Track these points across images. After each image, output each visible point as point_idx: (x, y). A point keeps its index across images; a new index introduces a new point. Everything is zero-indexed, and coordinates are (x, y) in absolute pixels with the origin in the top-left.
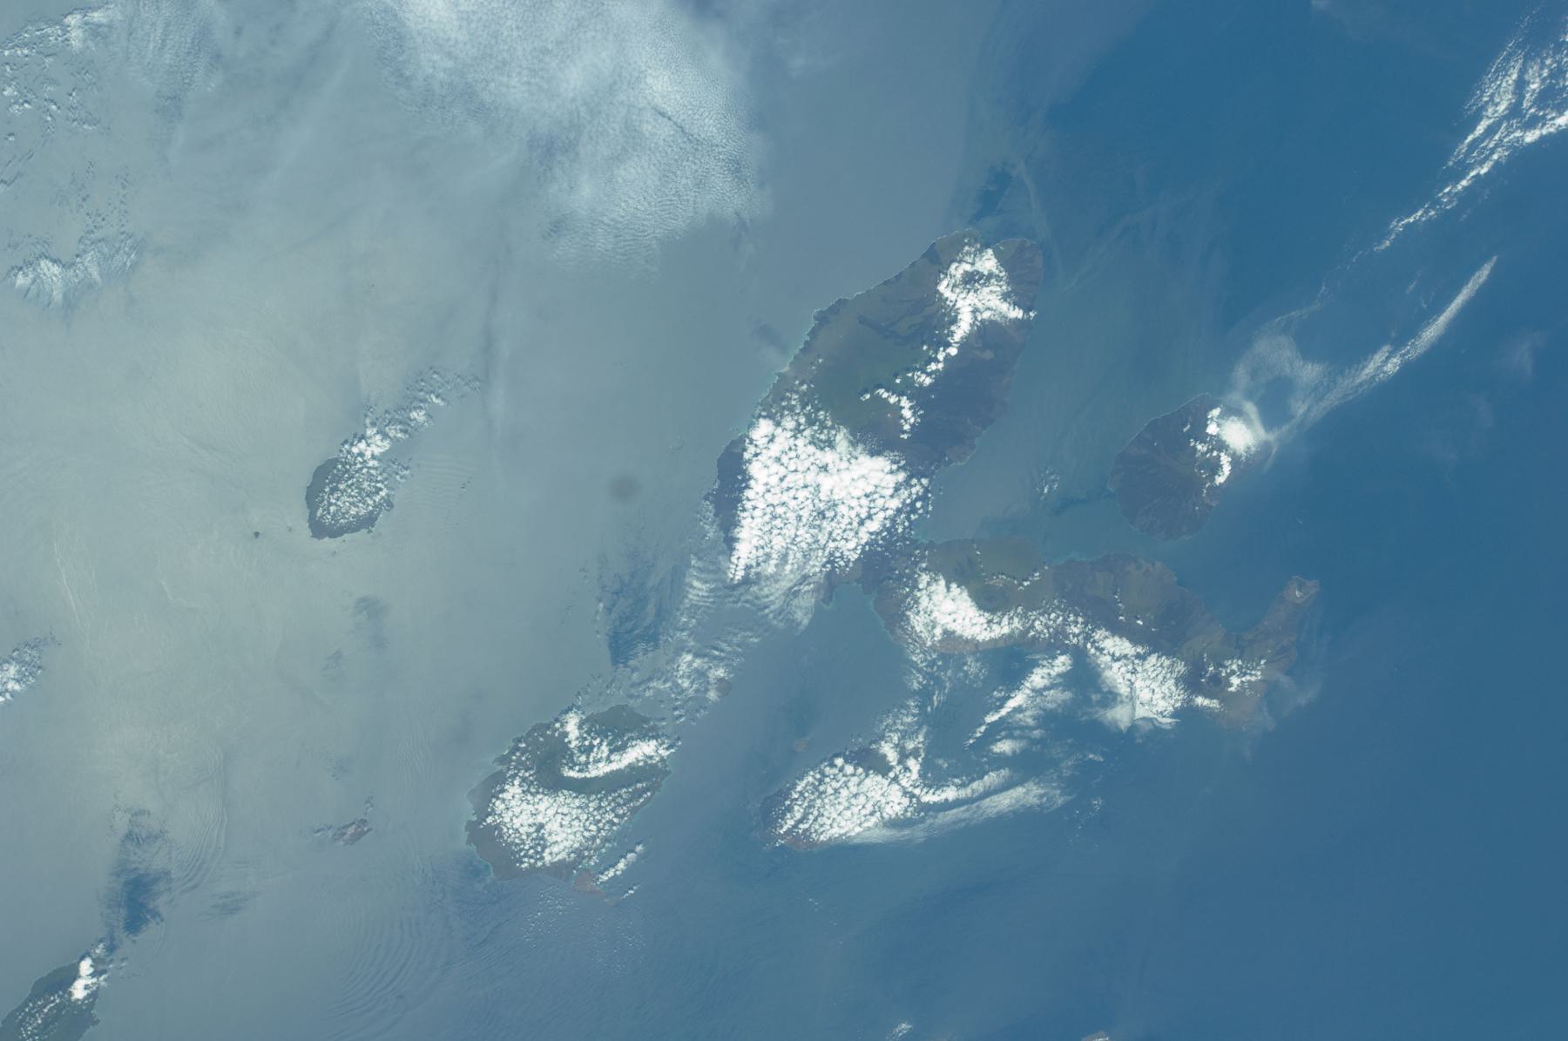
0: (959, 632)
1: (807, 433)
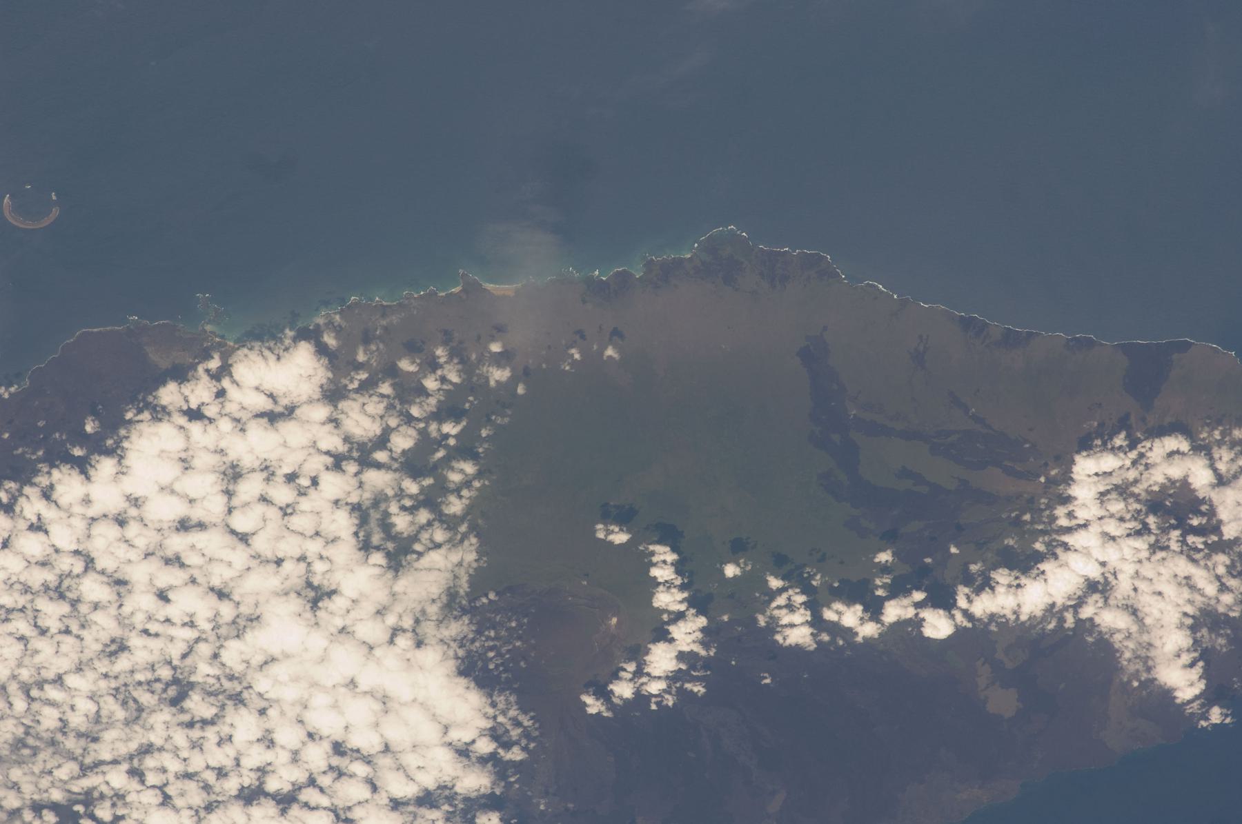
1: (375, 479)
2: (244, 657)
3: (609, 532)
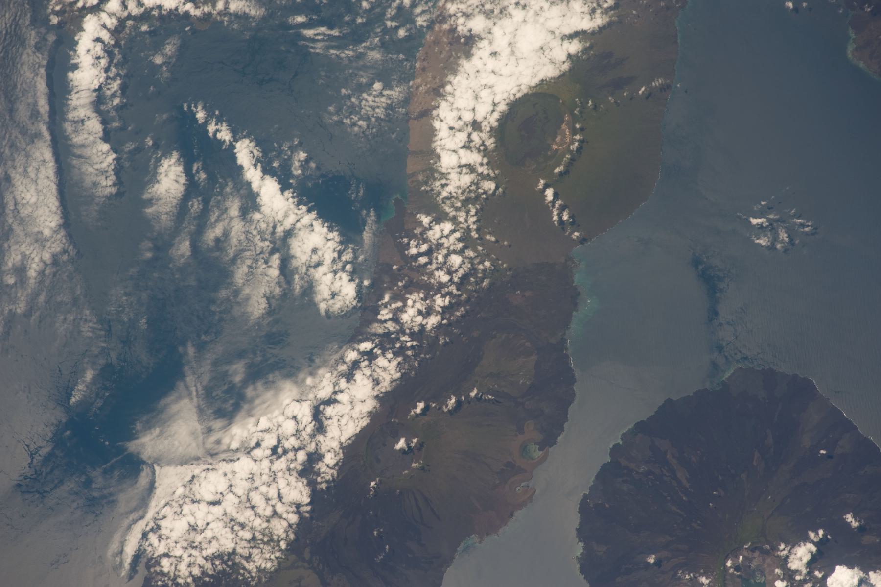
0: (466, 66)
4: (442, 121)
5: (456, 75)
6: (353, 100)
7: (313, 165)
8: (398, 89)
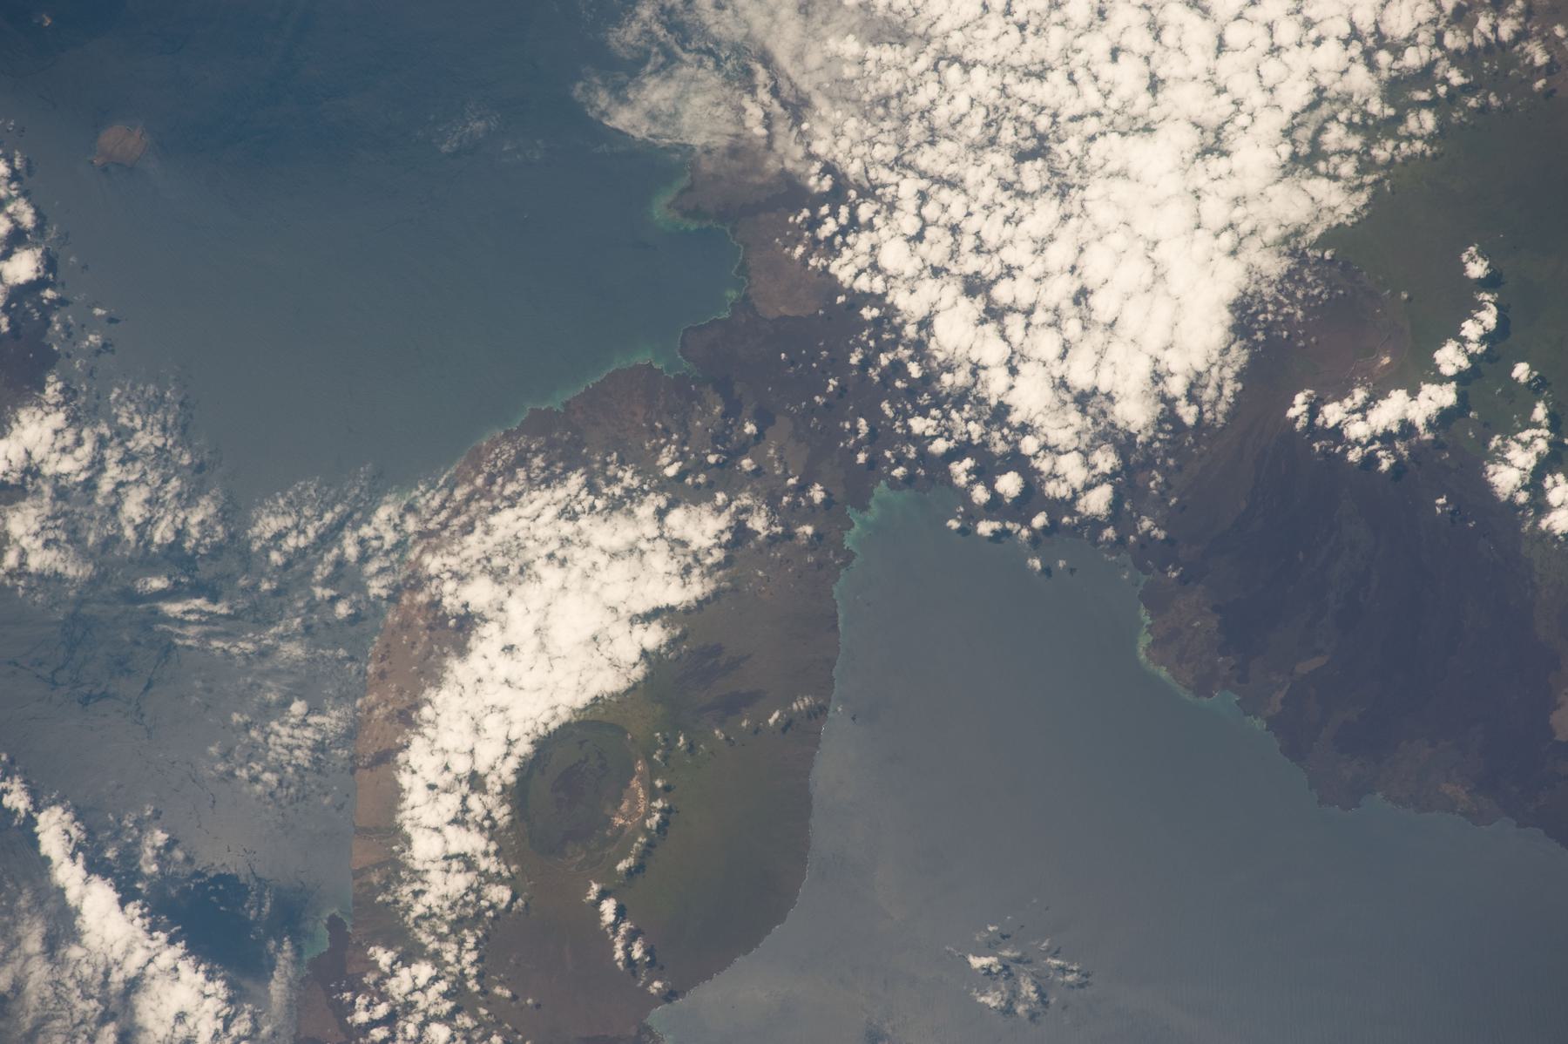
0: (458, 670)
2: (1109, 156)
3: (1472, 259)
4: (414, 772)
5: (440, 688)
6: (254, 734)
7: (178, 854)
8: (335, 714)
